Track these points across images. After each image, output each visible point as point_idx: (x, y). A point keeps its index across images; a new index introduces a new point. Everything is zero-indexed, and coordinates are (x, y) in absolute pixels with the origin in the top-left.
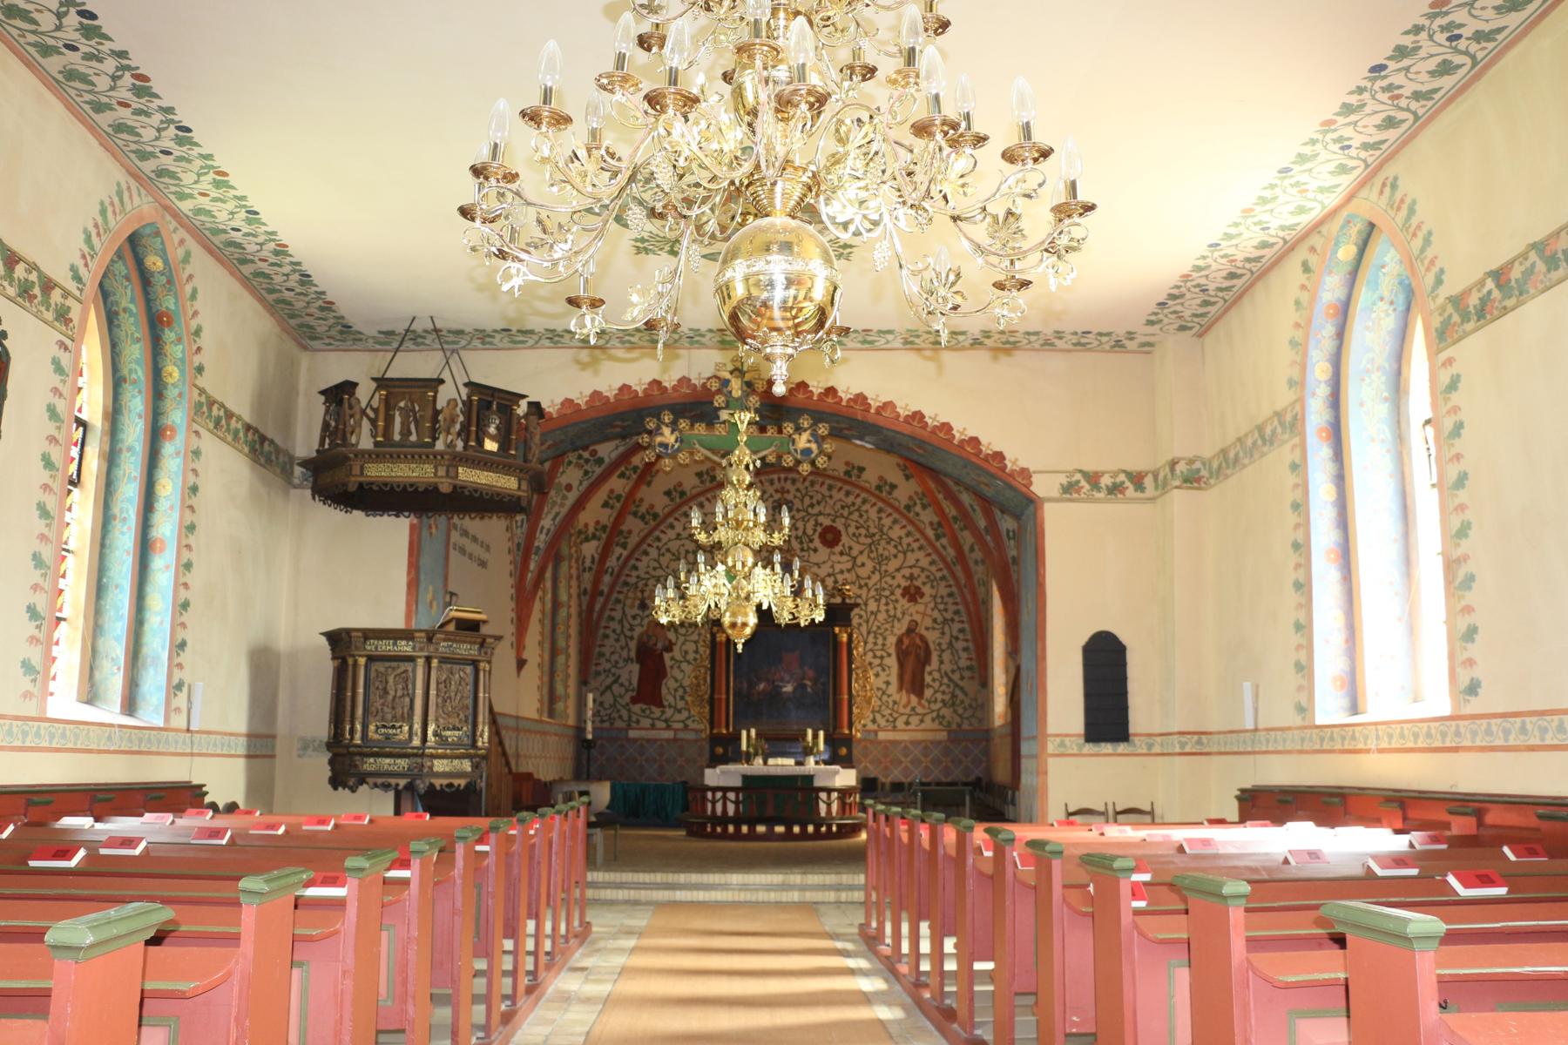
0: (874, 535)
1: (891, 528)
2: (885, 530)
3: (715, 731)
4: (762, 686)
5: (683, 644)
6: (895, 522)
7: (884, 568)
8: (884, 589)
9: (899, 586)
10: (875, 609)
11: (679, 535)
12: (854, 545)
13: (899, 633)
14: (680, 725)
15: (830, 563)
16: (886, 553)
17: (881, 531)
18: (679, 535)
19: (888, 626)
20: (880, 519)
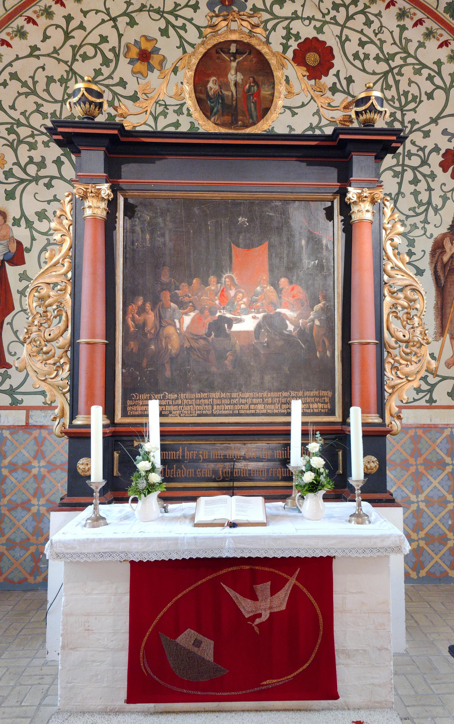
0: (392, 57)
1: (421, 45)
2: (411, 48)
3: (78, 422)
4: (187, 320)
5: (44, 249)
6: (429, 34)
7: (409, 117)
8: (410, 155)
9: (436, 149)
10: (394, 191)
11: (34, 48)
12: (357, 75)
13: (437, 233)
14: (38, 401)
15: (312, 107)
16: (414, 90)
17: (405, 50)
18: (34, 48)
19: (417, 220)
20: (403, 28)
